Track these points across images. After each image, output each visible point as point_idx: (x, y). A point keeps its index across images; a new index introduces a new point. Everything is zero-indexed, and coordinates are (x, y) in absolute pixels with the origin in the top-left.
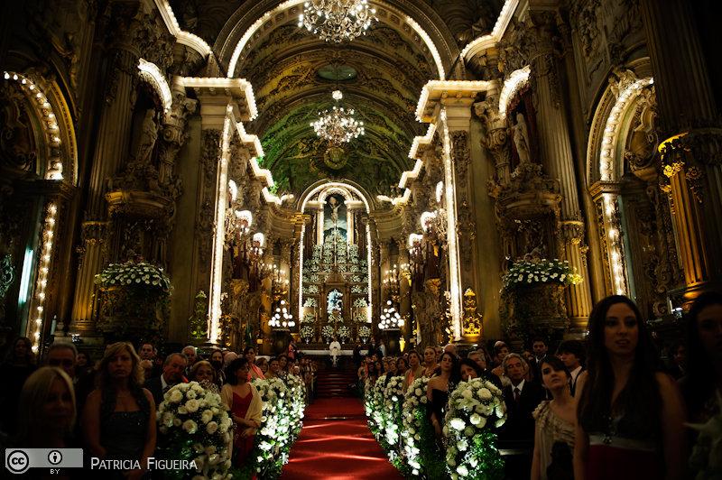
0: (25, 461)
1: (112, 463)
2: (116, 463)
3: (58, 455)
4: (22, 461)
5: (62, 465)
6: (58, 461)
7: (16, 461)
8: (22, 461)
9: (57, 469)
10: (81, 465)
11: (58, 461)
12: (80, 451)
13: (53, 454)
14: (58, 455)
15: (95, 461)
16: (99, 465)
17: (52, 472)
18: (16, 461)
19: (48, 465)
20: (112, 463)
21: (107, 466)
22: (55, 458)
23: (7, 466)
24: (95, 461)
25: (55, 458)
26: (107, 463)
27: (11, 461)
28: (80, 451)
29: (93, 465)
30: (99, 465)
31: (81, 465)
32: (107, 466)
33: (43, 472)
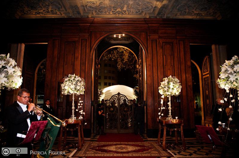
0: (8, 152)
1: (37, 152)
3: (17, 152)
4: (7, 152)
5: (20, 153)
6: (19, 152)
7: (5, 152)
8: (7, 152)
9: (19, 154)
10: (27, 153)
11: (19, 152)
12: (27, 148)
13: (17, 150)
14: (17, 152)
15: (31, 152)
16: (33, 153)
17: (17, 155)
18: (5, 152)
19: (16, 153)
22: (18, 151)
23: (2, 153)
24: (31, 152)
25: (18, 151)
26: (35, 152)
27: (3, 152)
28: (27, 148)
29: (31, 153)
30: (33, 153)
31: (27, 153)
33: (14, 155)
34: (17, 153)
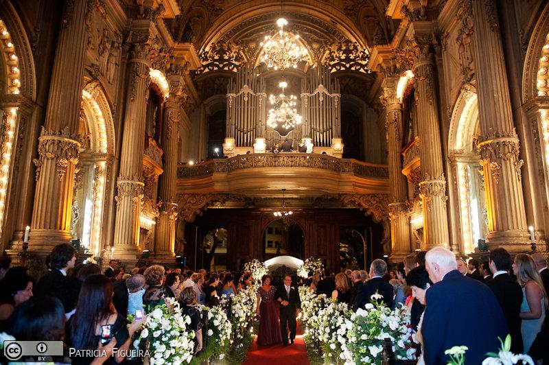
0: (19, 351)
1: (85, 352)
2: (88, 352)
3: (44, 346)
4: (16, 351)
5: (46, 354)
6: (44, 350)
7: (12, 351)
8: (16, 351)
9: (44, 356)
10: (61, 354)
11: (44, 350)
13: (40, 346)
14: (44, 346)
15: (72, 351)
16: (75, 354)
18: (12, 351)
20: (85, 352)
21: (81, 354)
22: (42, 348)
23: (5, 354)
24: (72, 351)
25: (42, 348)
26: (81, 352)
27: (8, 351)
29: (71, 353)
30: (75, 354)
31: (61, 354)
32: (81, 354)
34: (40, 354)
